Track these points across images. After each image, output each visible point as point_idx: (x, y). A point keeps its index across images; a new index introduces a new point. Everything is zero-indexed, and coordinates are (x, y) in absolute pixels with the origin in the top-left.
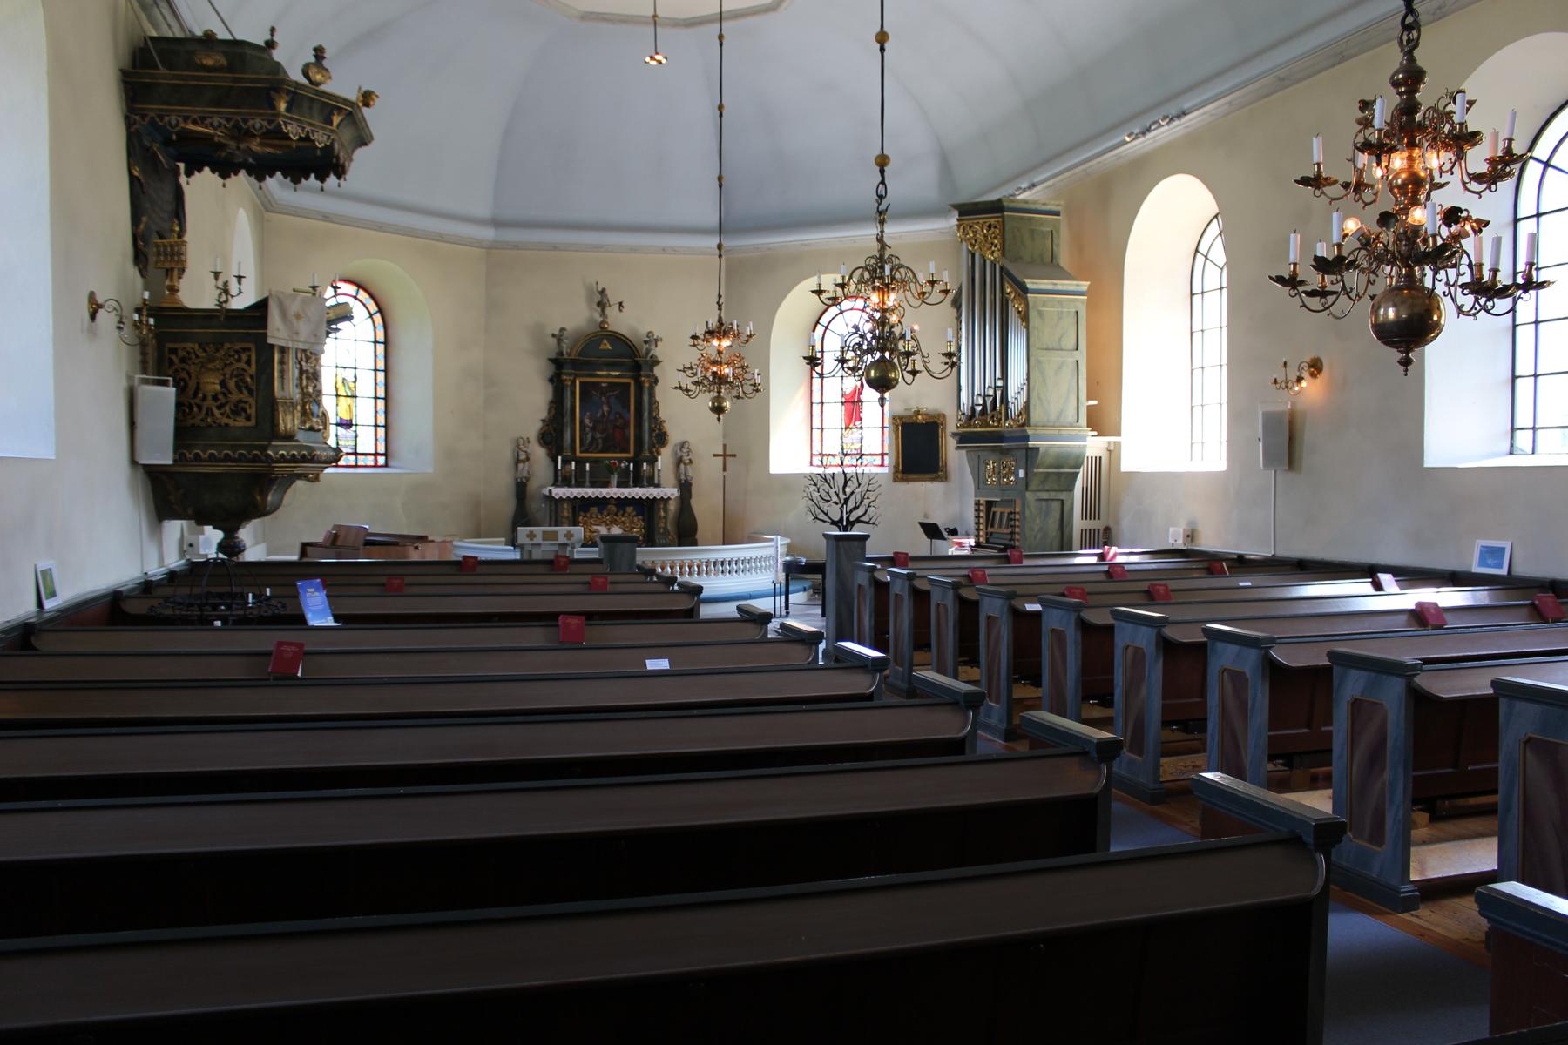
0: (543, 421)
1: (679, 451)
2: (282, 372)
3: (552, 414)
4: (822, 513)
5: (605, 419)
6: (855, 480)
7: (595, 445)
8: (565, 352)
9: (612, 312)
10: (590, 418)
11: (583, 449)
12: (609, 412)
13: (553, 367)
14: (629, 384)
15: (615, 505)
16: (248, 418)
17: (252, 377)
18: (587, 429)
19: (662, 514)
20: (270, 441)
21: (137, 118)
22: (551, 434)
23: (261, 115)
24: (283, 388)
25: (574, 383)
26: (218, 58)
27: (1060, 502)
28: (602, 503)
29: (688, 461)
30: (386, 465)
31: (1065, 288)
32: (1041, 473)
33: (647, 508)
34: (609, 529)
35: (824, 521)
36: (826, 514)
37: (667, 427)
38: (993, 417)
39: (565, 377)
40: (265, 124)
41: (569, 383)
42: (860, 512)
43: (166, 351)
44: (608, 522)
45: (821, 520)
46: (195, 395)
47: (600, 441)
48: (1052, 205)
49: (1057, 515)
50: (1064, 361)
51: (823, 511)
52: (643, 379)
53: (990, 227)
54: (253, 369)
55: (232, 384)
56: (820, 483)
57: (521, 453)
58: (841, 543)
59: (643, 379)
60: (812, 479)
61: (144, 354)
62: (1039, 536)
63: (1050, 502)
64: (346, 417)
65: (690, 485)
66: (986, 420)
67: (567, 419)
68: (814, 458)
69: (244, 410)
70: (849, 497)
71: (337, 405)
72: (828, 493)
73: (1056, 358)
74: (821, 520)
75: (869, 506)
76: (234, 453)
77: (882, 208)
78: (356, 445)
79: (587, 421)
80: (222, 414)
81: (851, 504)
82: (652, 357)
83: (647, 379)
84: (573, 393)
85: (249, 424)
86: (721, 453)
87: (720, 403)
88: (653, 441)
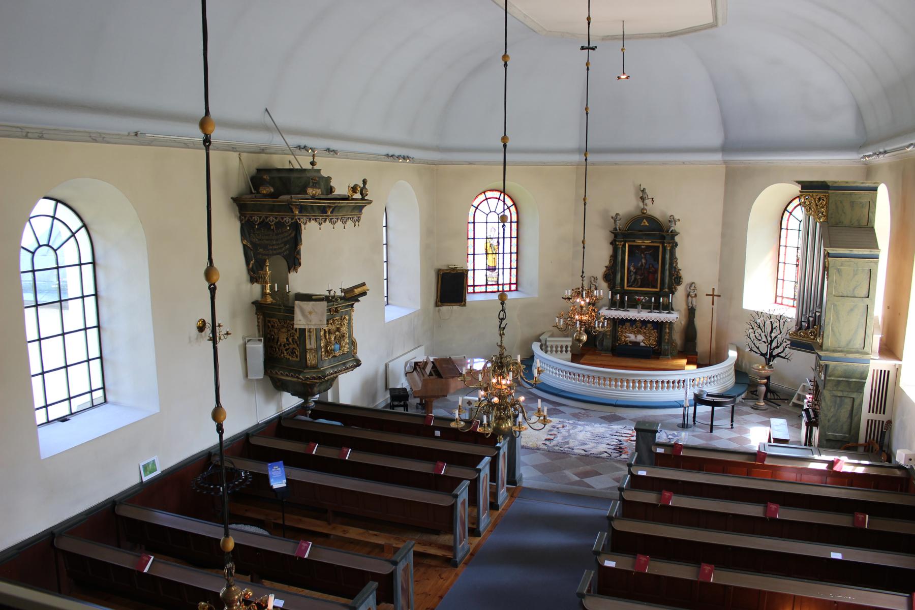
0: (606, 267)
1: (688, 289)
2: (310, 336)
3: (611, 264)
4: (755, 347)
5: (643, 267)
6: (778, 329)
8: (618, 229)
9: (648, 202)
10: (634, 267)
11: (629, 285)
12: (645, 264)
13: (613, 235)
14: (659, 247)
15: (641, 322)
16: (297, 357)
17: (298, 337)
18: (632, 273)
19: (667, 330)
20: (304, 370)
21: (243, 217)
22: (610, 274)
23: (289, 215)
24: (311, 344)
25: (624, 246)
26: (268, 190)
27: (852, 399)
28: (633, 322)
29: (694, 295)
30: (517, 290)
31: (860, 253)
32: (834, 380)
33: (659, 326)
34: (636, 336)
35: (757, 353)
36: (758, 348)
37: (682, 273)
38: (811, 333)
39: (617, 243)
40: (290, 220)
41: (621, 247)
42: (779, 350)
43: (267, 321)
44: (636, 333)
45: (754, 351)
46: (277, 342)
47: (639, 280)
48: (871, 183)
49: (849, 408)
50: (856, 305)
51: (756, 346)
52: (666, 245)
53: (819, 199)
54: (297, 335)
55: (290, 340)
56: (756, 328)
57: (592, 285)
58: (639, 433)
59: (666, 245)
60: (751, 325)
61: (258, 322)
62: (832, 421)
63: (843, 398)
64: (491, 264)
65: (695, 310)
66: (806, 334)
67: (619, 268)
68: (778, 298)
69: (295, 353)
70: (773, 340)
71: (487, 259)
72: (760, 335)
73: (849, 303)
74: (754, 351)
75: (786, 347)
76: (289, 374)
77: (503, 326)
78: (498, 279)
79: (632, 268)
80: (287, 353)
81: (774, 344)
82: (672, 232)
83: (668, 245)
84: (624, 252)
85: (297, 360)
86: (712, 294)
87: (579, 337)
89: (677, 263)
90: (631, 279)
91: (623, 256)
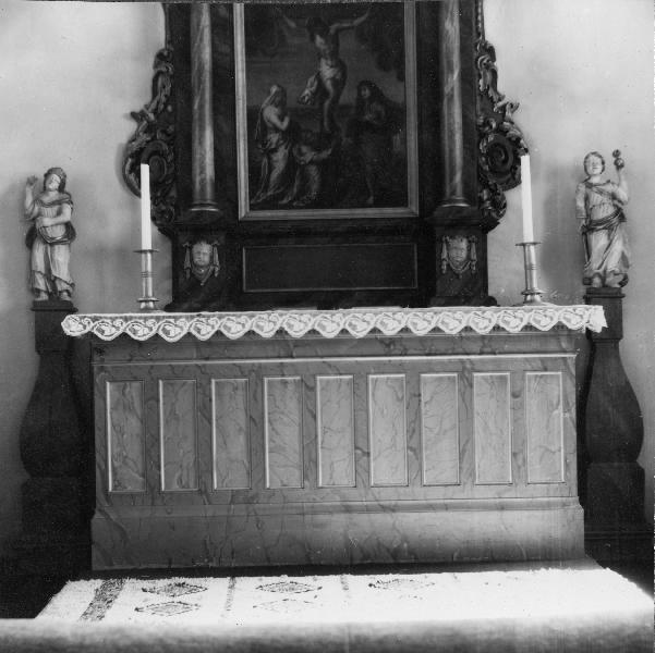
5: (327, 103)
7: (297, 183)
10: (281, 102)
12: (339, 84)
18: (274, 138)
37: (528, 122)
47: (313, 171)
79: (271, 114)
88: (479, 167)
89: (494, 73)
90: (271, 169)
91: (225, 49)
